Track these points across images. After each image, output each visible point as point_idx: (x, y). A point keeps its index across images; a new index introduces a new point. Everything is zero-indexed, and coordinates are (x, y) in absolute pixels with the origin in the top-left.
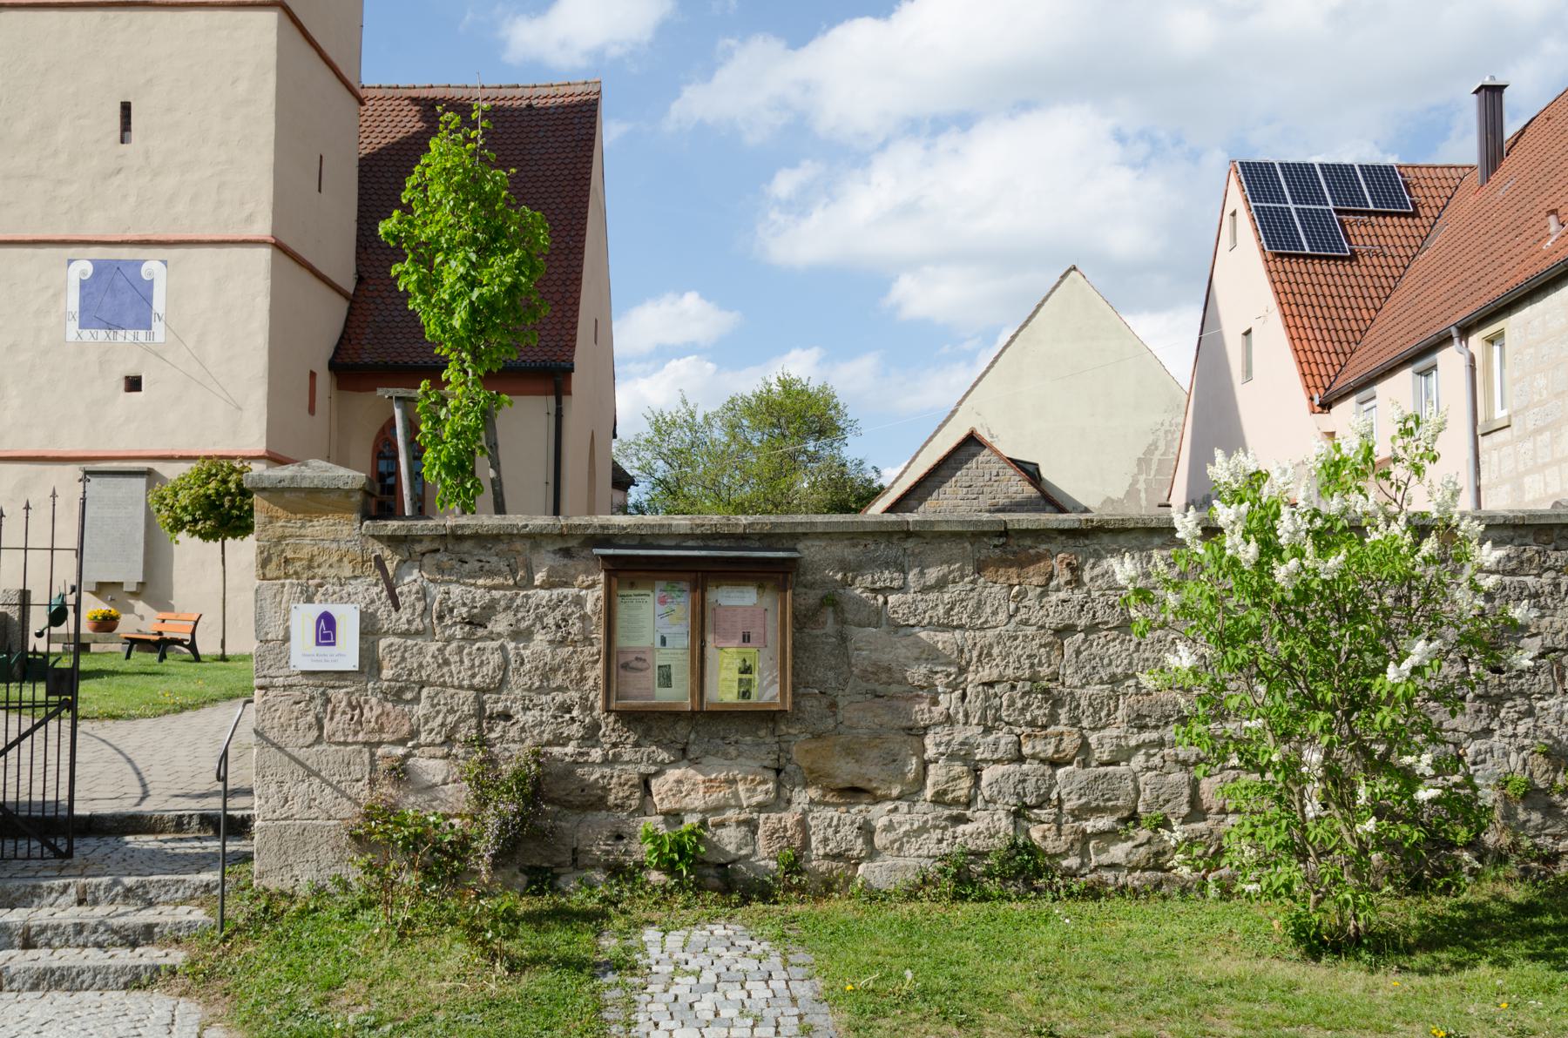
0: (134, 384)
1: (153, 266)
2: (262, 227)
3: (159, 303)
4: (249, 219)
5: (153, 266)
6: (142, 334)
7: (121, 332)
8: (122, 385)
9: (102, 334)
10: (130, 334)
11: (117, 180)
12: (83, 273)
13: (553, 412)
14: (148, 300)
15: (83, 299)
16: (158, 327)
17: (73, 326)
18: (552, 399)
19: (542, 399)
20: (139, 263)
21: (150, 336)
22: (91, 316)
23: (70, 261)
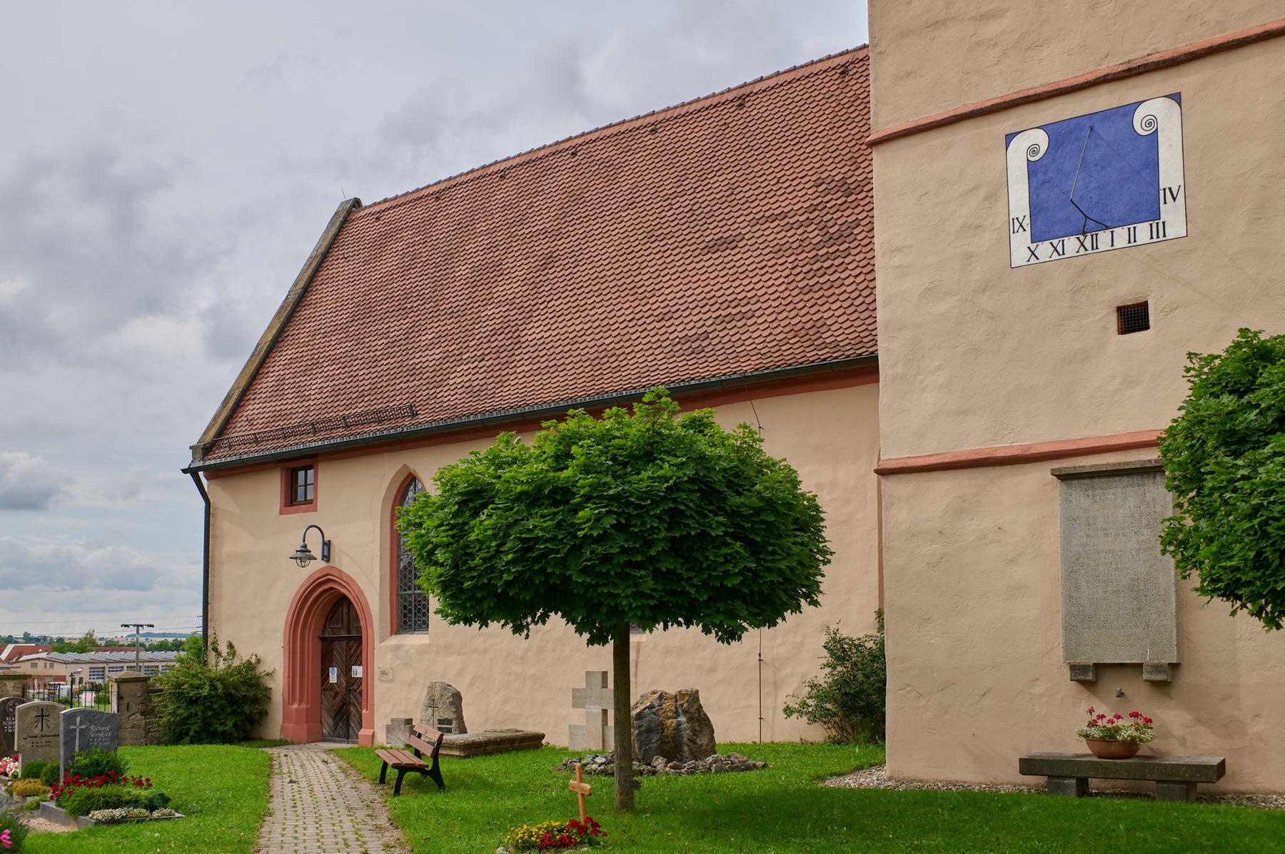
0: (1133, 318)
1: (1154, 110)
3: (1170, 173)
6: (1143, 230)
7: (1104, 236)
8: (1113, 321)
9: (1071, 244)
10: (1121, 234)
12: (1033, 150)
14: (1153, 165)
17: (1021, 241)
21: (1159, 232)
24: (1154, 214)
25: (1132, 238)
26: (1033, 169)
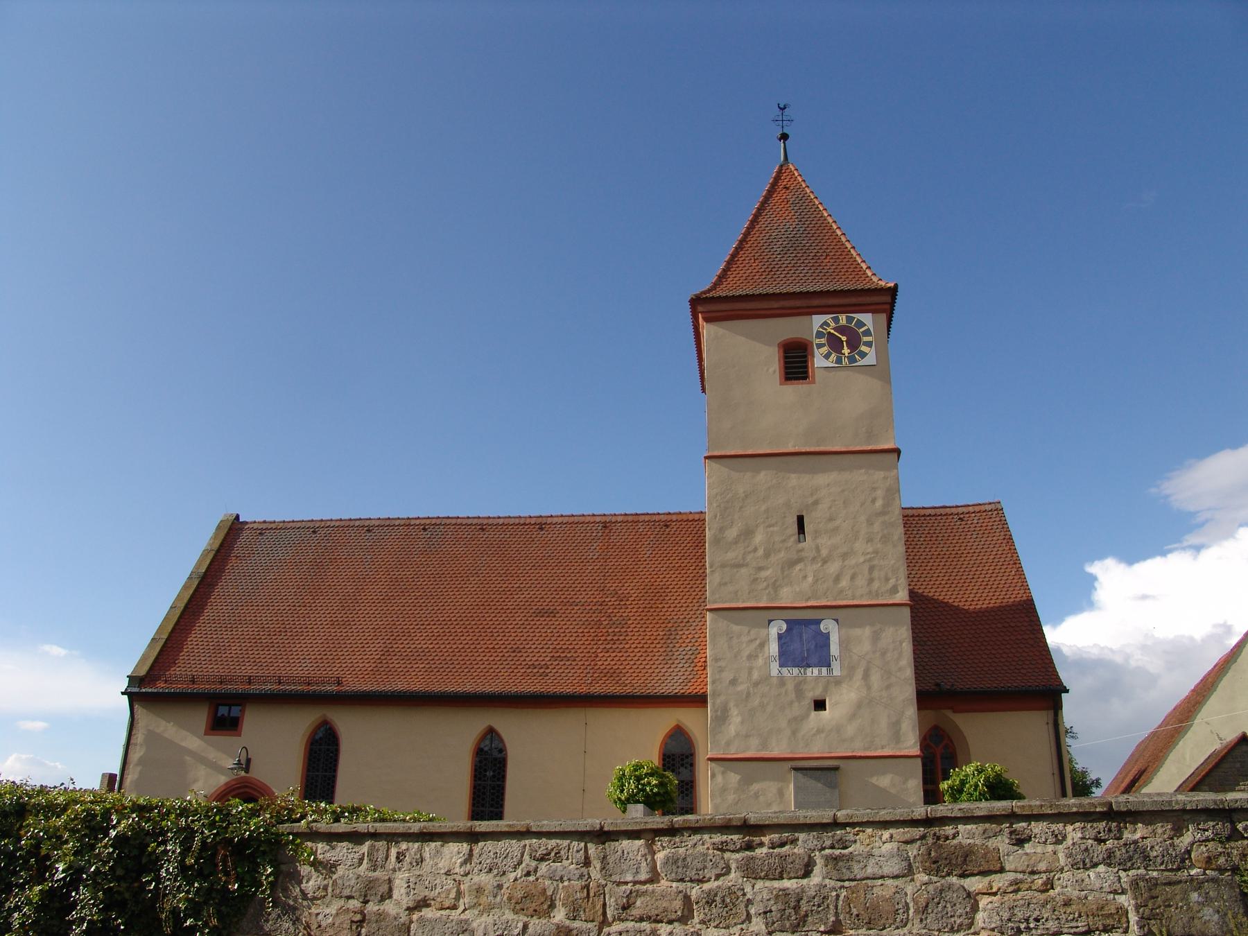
2: (902, 596)
3: (834, 649)
4: (894, 590)
5: (827, 625)
6: (824, 670)
9: (796, 671)
10: (816, 671)
11: (798, 567)
13: (1051, 722)
15: (781, 646)
16: (836, 665)
18: (1051, 713)
19: (1044, 713)
20: (818, 622)
22: (786, 658)
23: (770, 621)
24: (829, 665)
25: (820, 672)
26: (780, 637)
